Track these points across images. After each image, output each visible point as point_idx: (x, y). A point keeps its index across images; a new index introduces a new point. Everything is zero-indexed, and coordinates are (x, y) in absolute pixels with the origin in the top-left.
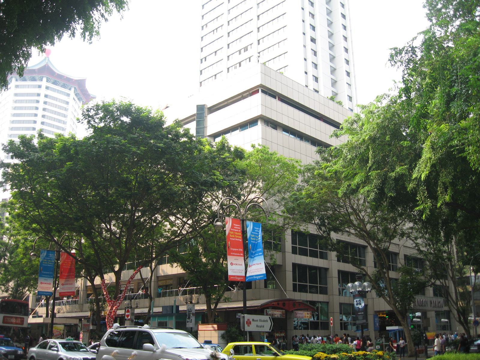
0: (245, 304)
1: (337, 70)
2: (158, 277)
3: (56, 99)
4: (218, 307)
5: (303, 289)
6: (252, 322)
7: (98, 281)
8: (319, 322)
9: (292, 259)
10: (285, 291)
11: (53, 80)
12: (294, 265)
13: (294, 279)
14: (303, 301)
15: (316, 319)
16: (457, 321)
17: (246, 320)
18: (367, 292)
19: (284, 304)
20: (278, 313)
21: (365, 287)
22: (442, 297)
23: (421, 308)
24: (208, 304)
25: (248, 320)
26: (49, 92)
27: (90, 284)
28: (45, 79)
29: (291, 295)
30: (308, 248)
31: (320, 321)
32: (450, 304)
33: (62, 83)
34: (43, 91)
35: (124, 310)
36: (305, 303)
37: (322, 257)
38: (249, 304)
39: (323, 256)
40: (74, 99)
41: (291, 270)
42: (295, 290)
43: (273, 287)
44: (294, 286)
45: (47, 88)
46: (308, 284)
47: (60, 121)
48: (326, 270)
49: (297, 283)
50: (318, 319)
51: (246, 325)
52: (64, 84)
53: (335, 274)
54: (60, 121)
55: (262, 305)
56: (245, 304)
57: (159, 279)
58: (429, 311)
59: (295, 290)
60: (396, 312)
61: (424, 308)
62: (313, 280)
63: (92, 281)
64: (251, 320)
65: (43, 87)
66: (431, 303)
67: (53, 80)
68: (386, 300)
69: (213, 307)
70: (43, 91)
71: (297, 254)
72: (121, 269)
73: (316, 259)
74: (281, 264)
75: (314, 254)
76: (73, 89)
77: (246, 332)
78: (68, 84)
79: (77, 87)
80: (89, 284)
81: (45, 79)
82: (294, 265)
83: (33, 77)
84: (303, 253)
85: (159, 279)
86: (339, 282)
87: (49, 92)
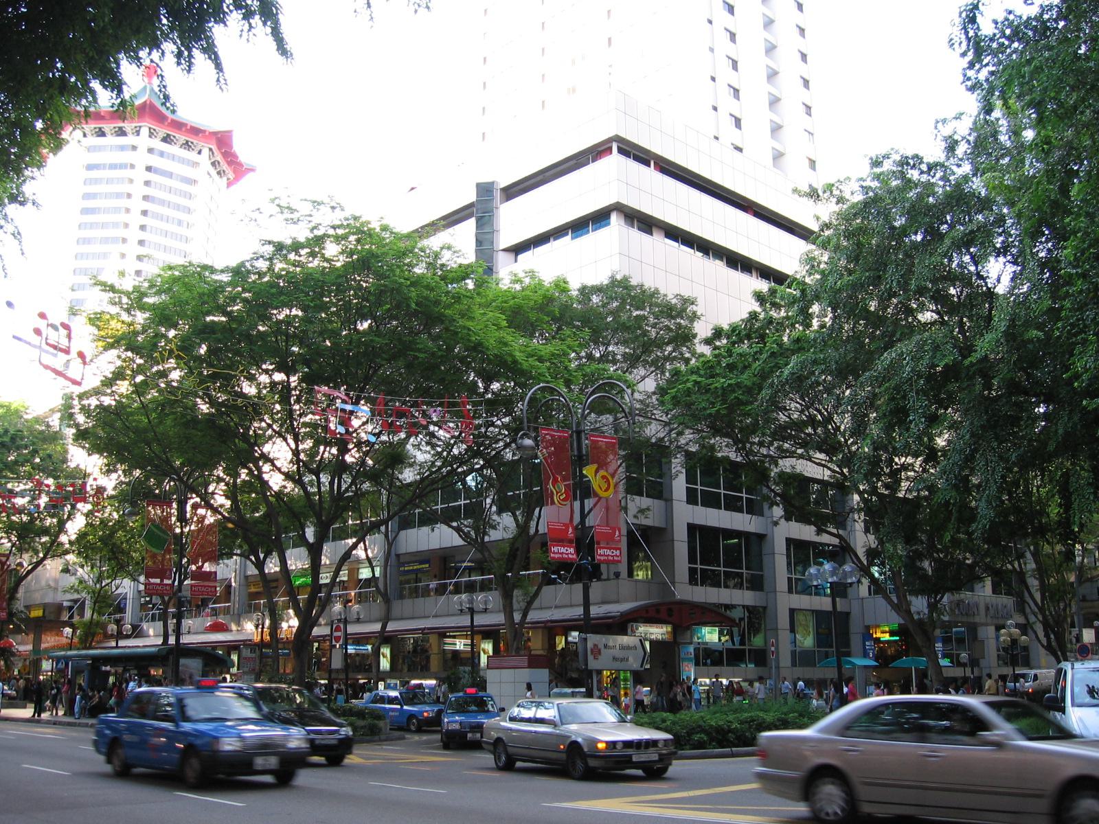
0: (587, 610)
1: (778, 49)
2: (398, 556)
3: (170, 175)
4: (529, 619)
5: (710, 579)
6: (603, 650)
7: (272, 567)
8: (744, 650)
9: (686, 514)
10: (673, 583)
11: (162, 132)
12: (692, 528)
13: (692, 559)
14: (711, 604)
15: (737, 639)
16: (1043, 646)
17: (590, 645)
18: (851, 584)
19: (670, 610)
20: (658, 632)
21: (845, 574)
22: (1012, 595)
23: (964, 619)
24: (508, 610)
25: (595, 645)
26: (155, 161)
27: (256, 572)
28: (145, 131)
29: (685, 592)
30: (722, 491)
31: (747, 647)
32: (1028, 610)
33: (182, 138)
34: (142, 153)
35: (329, 628)
36: (715, 609)
37: (751, 511)
38: (595, 611)
39: (753, 509)
40: (209, 174)
41: (686, 539)
42: (693, 581)
43: (647, 575)
44: (692, 572)
45: (150, 151)
46: (722, 569)
47: (178, 207)
48: (761, 537)
49: (699, 566)
50: (742, 643)
51: (590, 657)
52: (187, 142)
53: (780, 547)
54: (178, 207)
55: (623, 614)
56: (587, 610)
57: (402, 560)
58: (983, 625)
59: (693, 581)
60: (911, 629)
61: (971, 620)
62: (733, 559)
63: (260, 565)
64: (601, 646)
65: (142, 149)
66: (987, 609)
67: (162, 132)
68: (889, 601)
69: (517, 617)
70: (142, 153)
71: (697, 504)
72: (322, 538)
73: (740, 515)
74: (663, 526)
75: (733, 505)
76: (206, 152)
77: (591, 672)
78: (195, 142)
79: (214, 147)
80: (252, 571)
81: (145, 131)
82: (692, 528)
83: (120, 128)
84: (711, 501)
85: (402, 560)
86: (789, 564)
87: (155, 161)
